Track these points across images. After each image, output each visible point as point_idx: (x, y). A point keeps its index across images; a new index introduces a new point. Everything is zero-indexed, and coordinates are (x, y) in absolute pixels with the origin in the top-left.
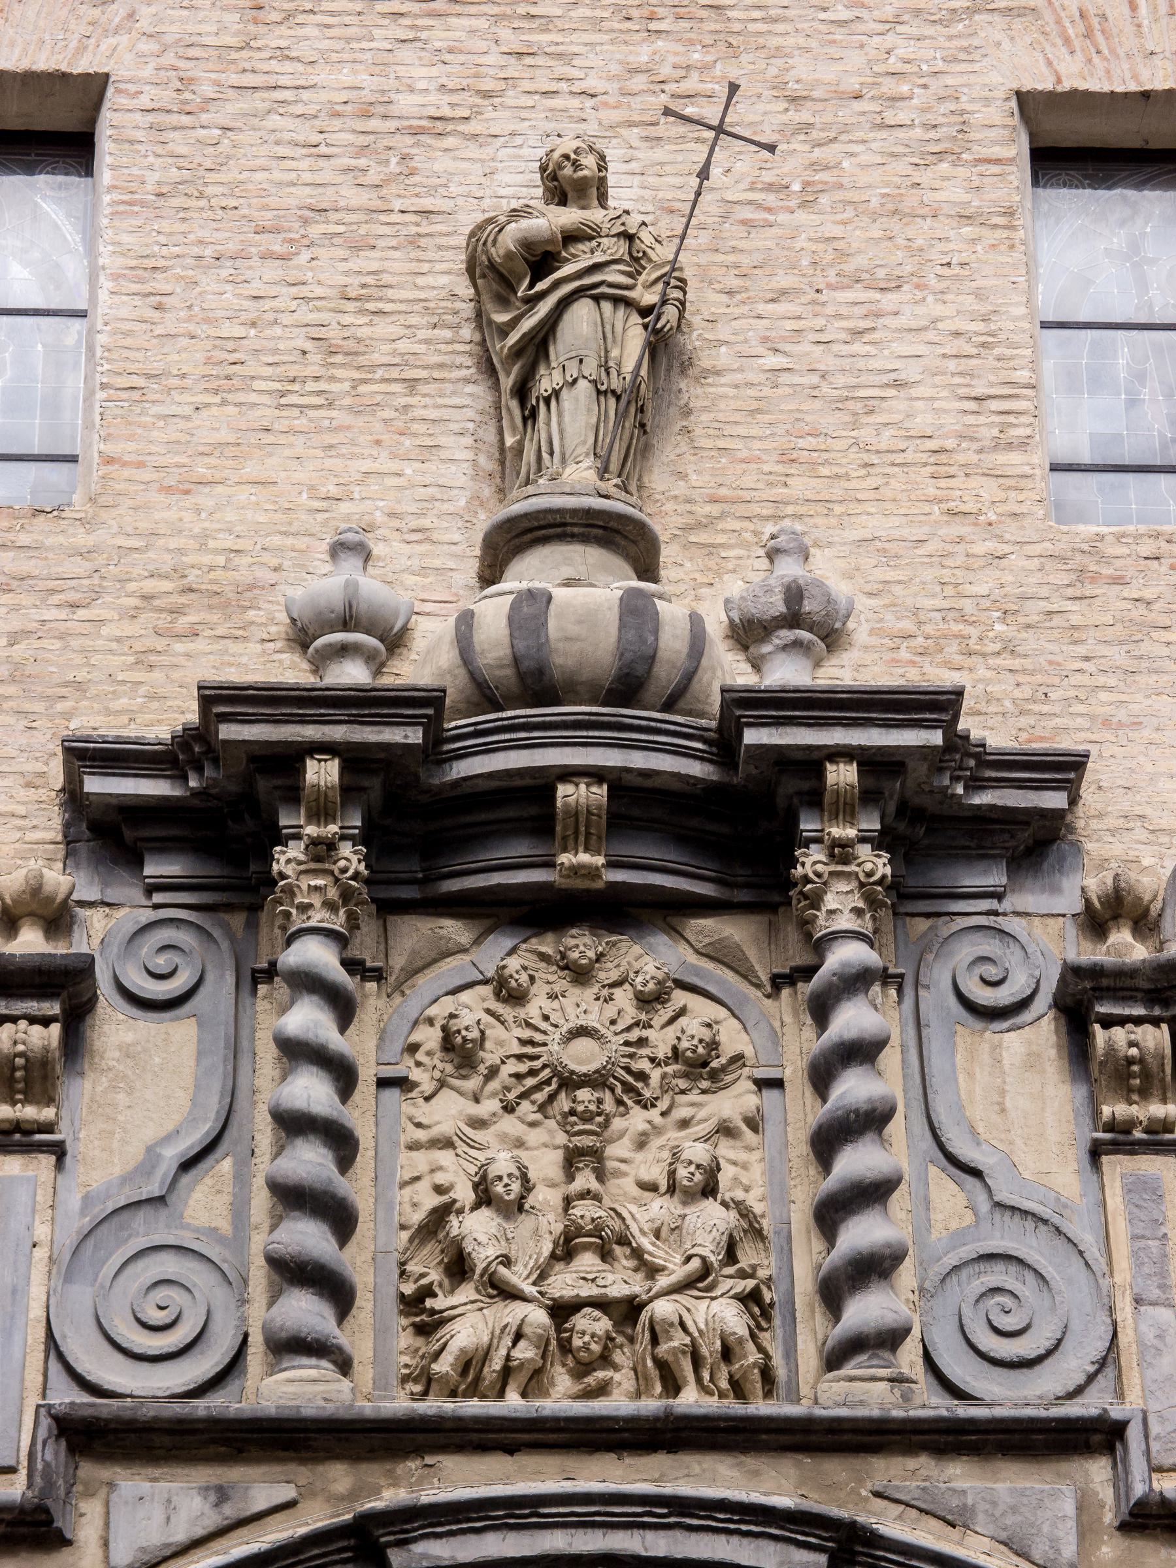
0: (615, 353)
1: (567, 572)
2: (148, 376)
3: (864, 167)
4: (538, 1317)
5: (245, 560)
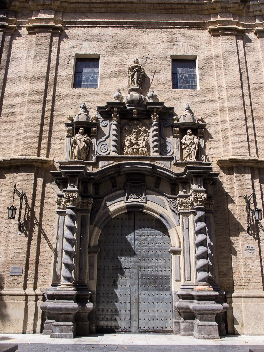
4: (132, 149)
5: (110, 92)
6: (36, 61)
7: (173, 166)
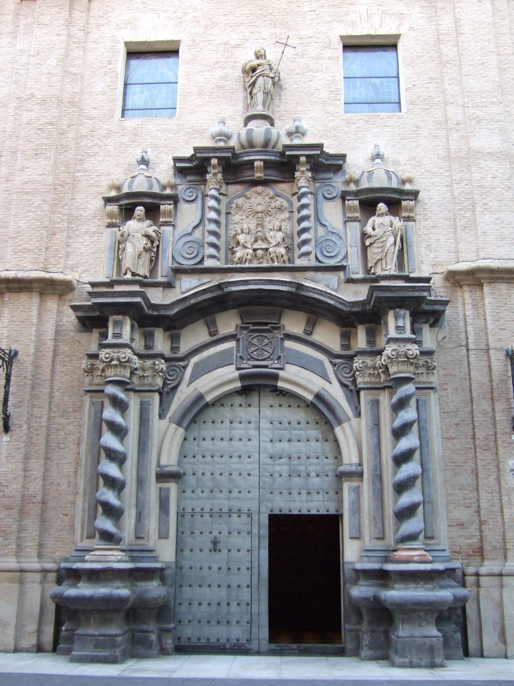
0: (266, 86)
1: (257, 125)
2: (187, 93)
3: (313, 50)
4: (251, 251)
6: (38, 62)
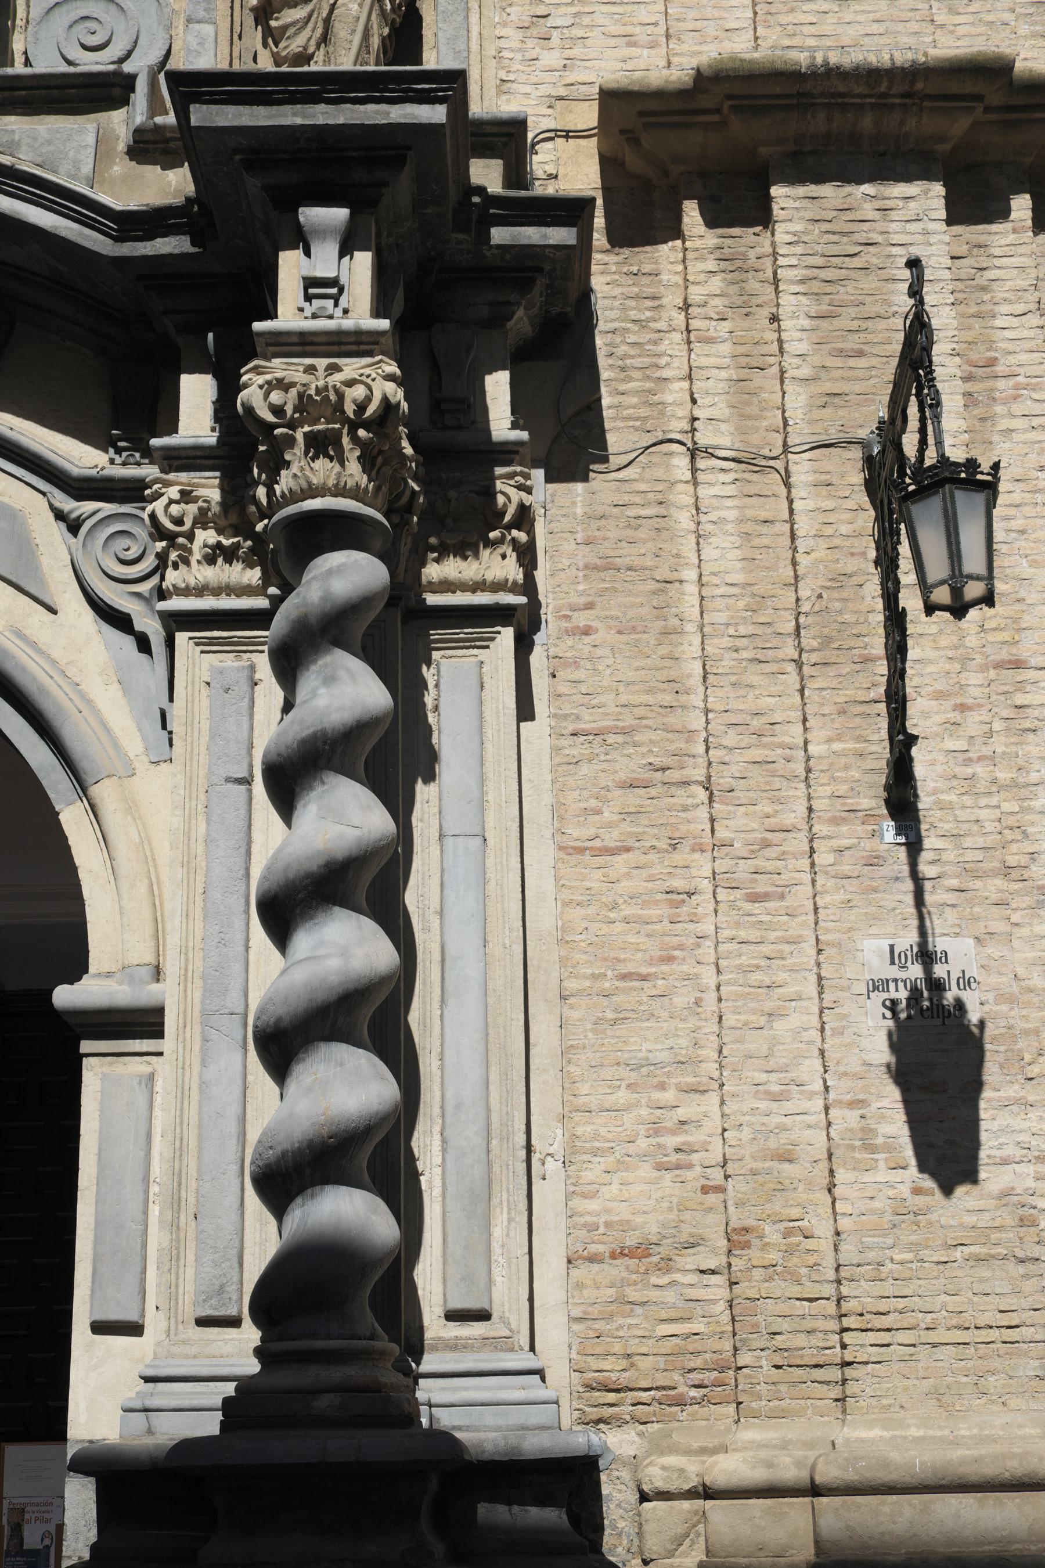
7: (121, 167)
